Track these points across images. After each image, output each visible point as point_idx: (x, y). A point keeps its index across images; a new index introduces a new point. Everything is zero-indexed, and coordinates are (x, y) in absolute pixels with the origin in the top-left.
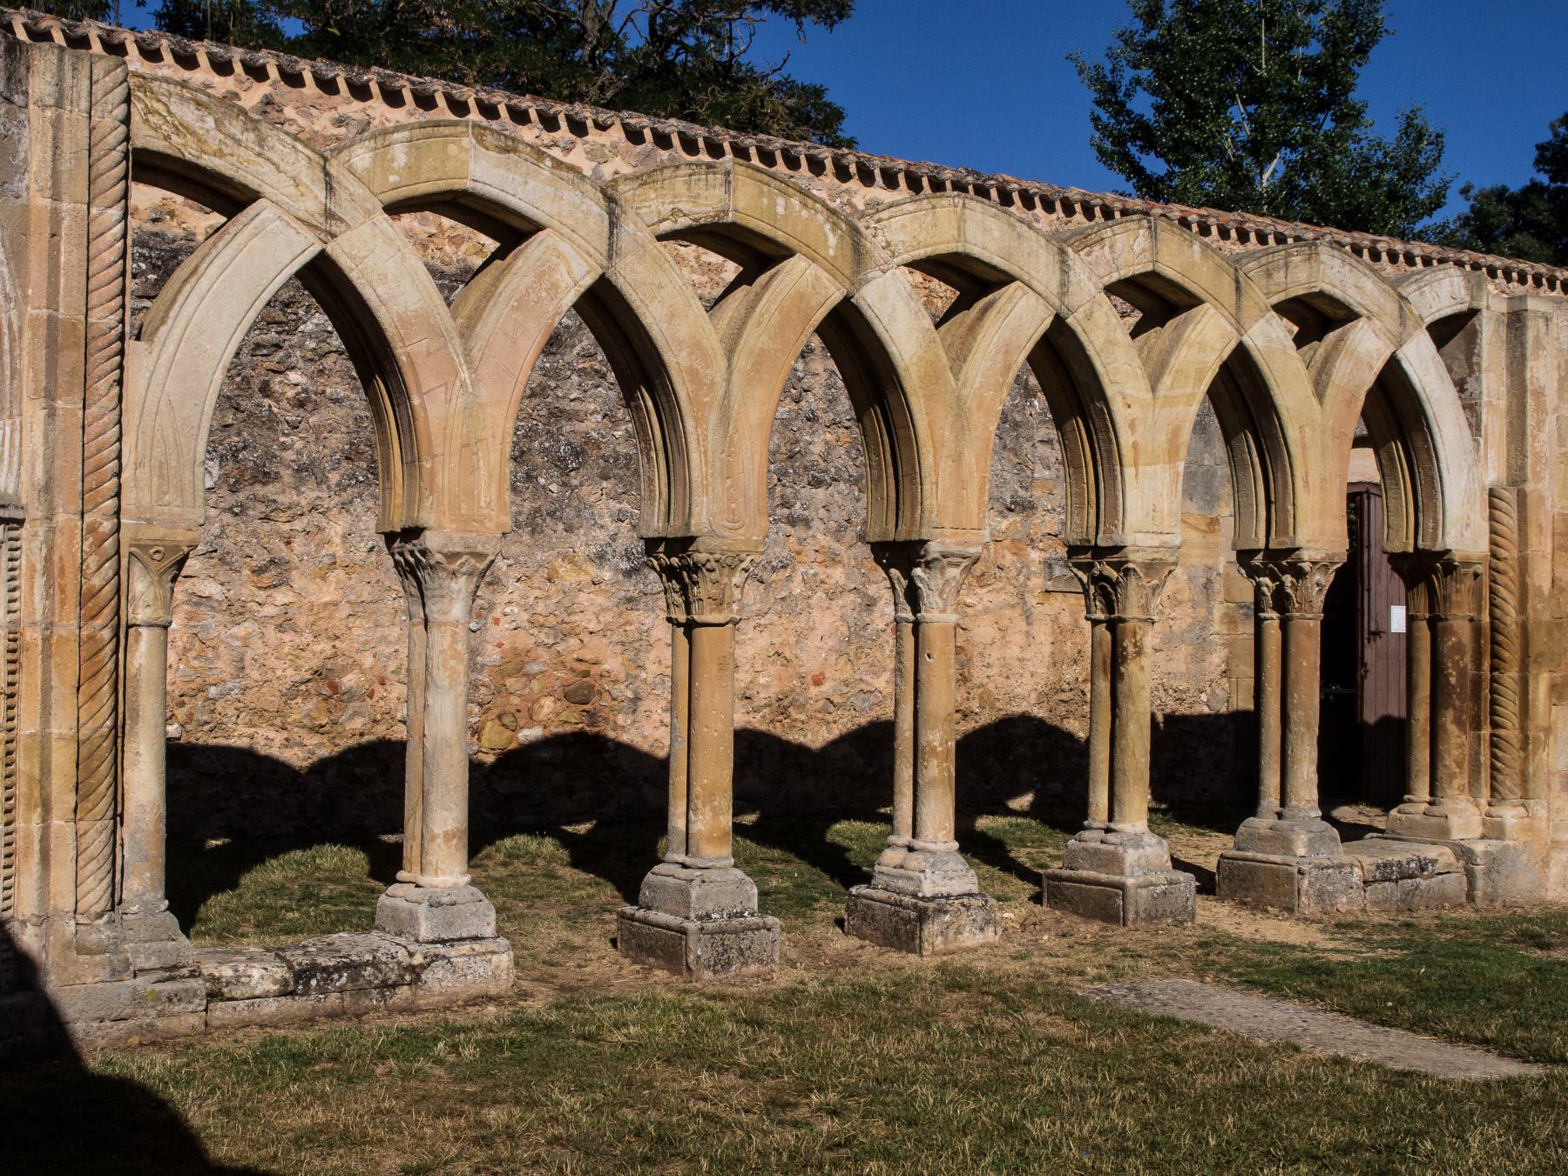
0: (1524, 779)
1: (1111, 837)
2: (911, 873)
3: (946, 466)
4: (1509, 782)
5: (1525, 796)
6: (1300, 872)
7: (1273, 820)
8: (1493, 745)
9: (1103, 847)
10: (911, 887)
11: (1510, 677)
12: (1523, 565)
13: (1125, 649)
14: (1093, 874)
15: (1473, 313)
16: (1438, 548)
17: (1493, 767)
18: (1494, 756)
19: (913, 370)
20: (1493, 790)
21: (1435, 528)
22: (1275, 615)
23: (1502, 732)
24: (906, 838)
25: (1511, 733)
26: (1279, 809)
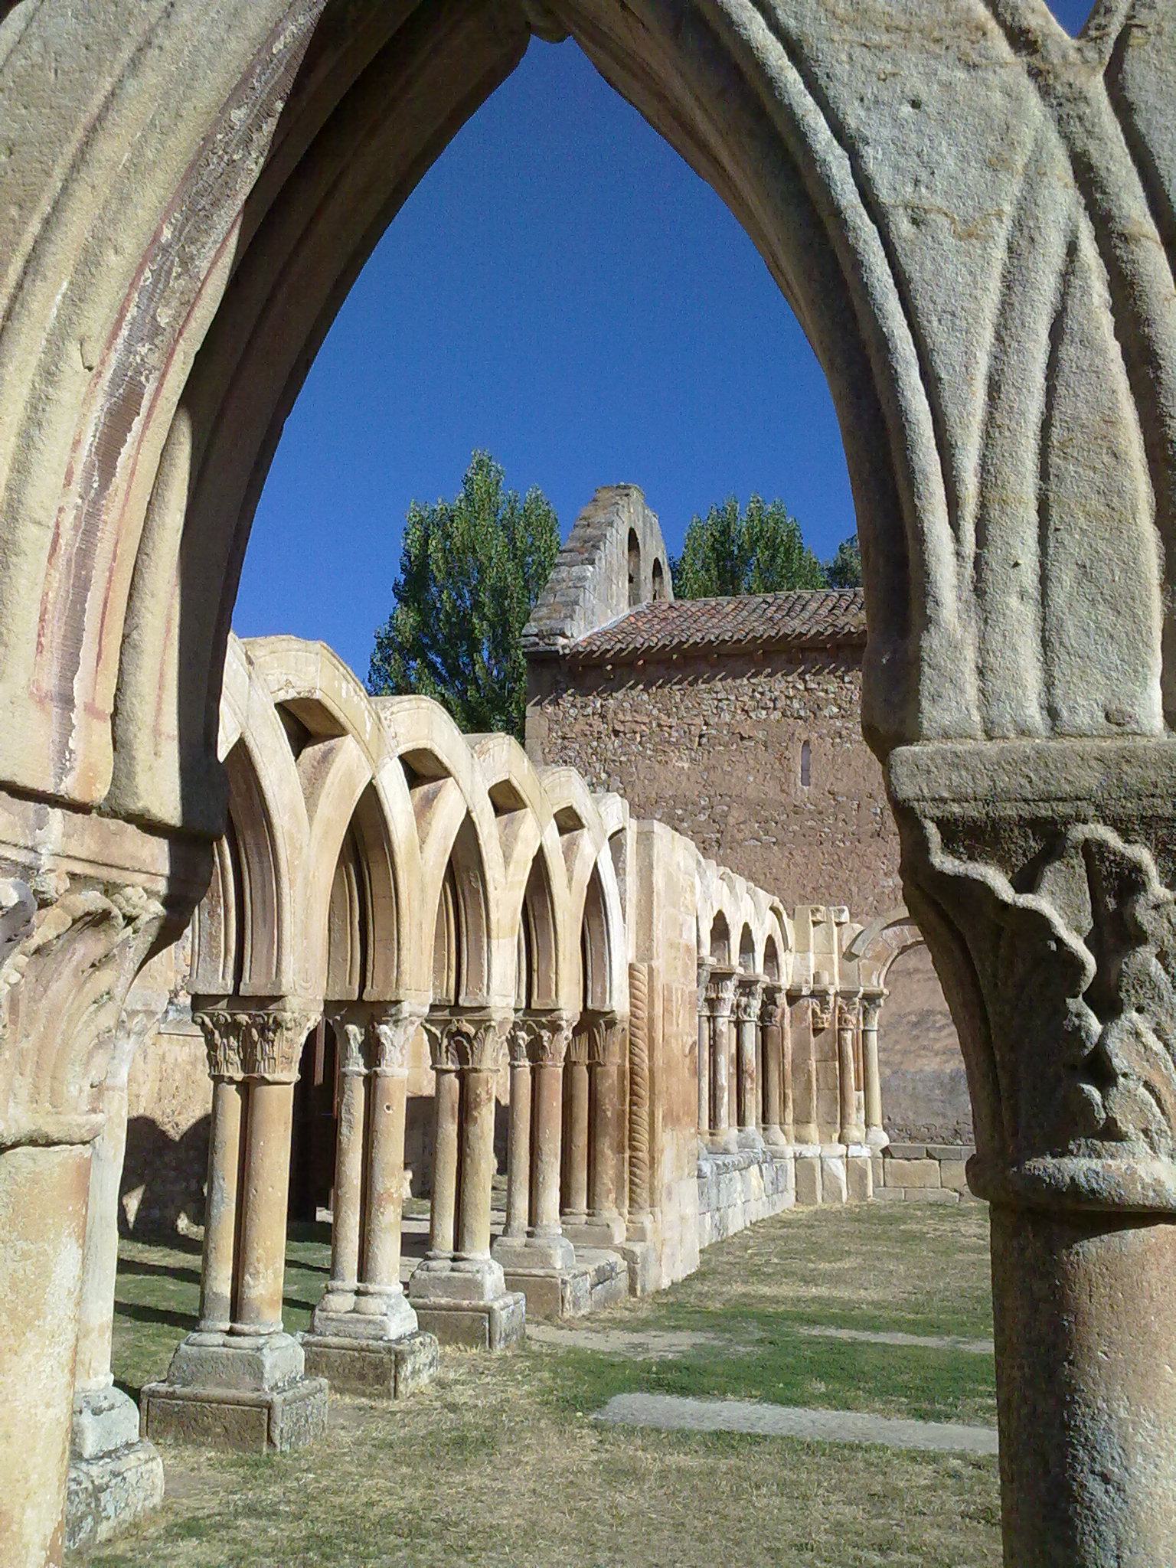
0: (652, 1190)
1: (461, 1264)
2: (371, 1317)
3: (415, 931)
4: (643, 1195)
5: (652, 1206)
6: (564, 1282)
7: (524, 1239)
8: (632, 1165)
9: (455, 1274)
10: (371, 1330)
11: (644, 1112)
12: (651, 1020)
13: (479, 1096)
14: (443, 1301)
15: (622, 830)
16: (607, 1009)
17: (632, 1182)
18: (632, 1173)
19: (403, 846)
20: (631, 1199)
21: (604, 993)
22: (527, 1063)
23: (640, 1154)
24: (352, 1282)
25: (644, 1155)
26: (527, 1229)
